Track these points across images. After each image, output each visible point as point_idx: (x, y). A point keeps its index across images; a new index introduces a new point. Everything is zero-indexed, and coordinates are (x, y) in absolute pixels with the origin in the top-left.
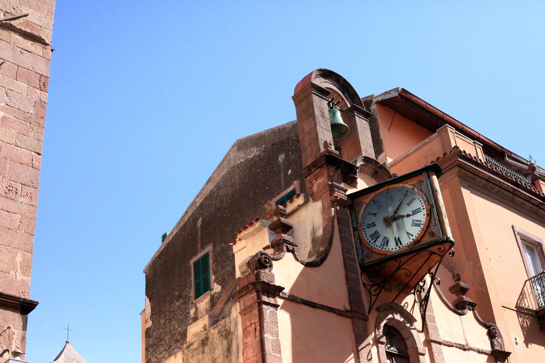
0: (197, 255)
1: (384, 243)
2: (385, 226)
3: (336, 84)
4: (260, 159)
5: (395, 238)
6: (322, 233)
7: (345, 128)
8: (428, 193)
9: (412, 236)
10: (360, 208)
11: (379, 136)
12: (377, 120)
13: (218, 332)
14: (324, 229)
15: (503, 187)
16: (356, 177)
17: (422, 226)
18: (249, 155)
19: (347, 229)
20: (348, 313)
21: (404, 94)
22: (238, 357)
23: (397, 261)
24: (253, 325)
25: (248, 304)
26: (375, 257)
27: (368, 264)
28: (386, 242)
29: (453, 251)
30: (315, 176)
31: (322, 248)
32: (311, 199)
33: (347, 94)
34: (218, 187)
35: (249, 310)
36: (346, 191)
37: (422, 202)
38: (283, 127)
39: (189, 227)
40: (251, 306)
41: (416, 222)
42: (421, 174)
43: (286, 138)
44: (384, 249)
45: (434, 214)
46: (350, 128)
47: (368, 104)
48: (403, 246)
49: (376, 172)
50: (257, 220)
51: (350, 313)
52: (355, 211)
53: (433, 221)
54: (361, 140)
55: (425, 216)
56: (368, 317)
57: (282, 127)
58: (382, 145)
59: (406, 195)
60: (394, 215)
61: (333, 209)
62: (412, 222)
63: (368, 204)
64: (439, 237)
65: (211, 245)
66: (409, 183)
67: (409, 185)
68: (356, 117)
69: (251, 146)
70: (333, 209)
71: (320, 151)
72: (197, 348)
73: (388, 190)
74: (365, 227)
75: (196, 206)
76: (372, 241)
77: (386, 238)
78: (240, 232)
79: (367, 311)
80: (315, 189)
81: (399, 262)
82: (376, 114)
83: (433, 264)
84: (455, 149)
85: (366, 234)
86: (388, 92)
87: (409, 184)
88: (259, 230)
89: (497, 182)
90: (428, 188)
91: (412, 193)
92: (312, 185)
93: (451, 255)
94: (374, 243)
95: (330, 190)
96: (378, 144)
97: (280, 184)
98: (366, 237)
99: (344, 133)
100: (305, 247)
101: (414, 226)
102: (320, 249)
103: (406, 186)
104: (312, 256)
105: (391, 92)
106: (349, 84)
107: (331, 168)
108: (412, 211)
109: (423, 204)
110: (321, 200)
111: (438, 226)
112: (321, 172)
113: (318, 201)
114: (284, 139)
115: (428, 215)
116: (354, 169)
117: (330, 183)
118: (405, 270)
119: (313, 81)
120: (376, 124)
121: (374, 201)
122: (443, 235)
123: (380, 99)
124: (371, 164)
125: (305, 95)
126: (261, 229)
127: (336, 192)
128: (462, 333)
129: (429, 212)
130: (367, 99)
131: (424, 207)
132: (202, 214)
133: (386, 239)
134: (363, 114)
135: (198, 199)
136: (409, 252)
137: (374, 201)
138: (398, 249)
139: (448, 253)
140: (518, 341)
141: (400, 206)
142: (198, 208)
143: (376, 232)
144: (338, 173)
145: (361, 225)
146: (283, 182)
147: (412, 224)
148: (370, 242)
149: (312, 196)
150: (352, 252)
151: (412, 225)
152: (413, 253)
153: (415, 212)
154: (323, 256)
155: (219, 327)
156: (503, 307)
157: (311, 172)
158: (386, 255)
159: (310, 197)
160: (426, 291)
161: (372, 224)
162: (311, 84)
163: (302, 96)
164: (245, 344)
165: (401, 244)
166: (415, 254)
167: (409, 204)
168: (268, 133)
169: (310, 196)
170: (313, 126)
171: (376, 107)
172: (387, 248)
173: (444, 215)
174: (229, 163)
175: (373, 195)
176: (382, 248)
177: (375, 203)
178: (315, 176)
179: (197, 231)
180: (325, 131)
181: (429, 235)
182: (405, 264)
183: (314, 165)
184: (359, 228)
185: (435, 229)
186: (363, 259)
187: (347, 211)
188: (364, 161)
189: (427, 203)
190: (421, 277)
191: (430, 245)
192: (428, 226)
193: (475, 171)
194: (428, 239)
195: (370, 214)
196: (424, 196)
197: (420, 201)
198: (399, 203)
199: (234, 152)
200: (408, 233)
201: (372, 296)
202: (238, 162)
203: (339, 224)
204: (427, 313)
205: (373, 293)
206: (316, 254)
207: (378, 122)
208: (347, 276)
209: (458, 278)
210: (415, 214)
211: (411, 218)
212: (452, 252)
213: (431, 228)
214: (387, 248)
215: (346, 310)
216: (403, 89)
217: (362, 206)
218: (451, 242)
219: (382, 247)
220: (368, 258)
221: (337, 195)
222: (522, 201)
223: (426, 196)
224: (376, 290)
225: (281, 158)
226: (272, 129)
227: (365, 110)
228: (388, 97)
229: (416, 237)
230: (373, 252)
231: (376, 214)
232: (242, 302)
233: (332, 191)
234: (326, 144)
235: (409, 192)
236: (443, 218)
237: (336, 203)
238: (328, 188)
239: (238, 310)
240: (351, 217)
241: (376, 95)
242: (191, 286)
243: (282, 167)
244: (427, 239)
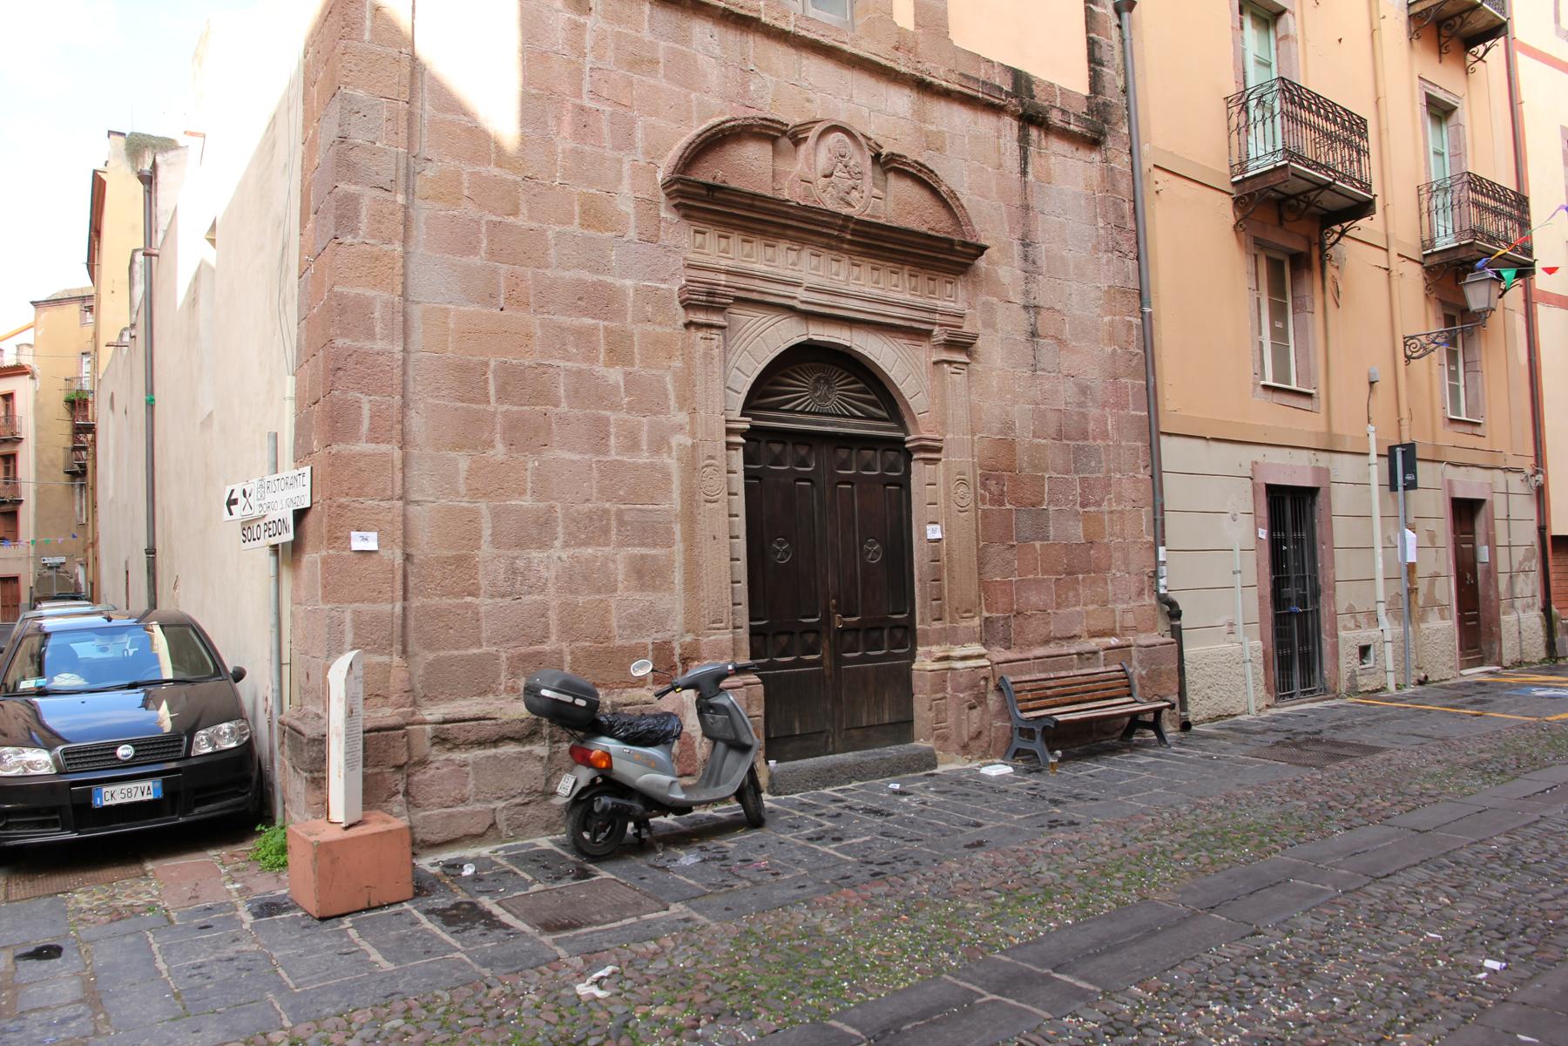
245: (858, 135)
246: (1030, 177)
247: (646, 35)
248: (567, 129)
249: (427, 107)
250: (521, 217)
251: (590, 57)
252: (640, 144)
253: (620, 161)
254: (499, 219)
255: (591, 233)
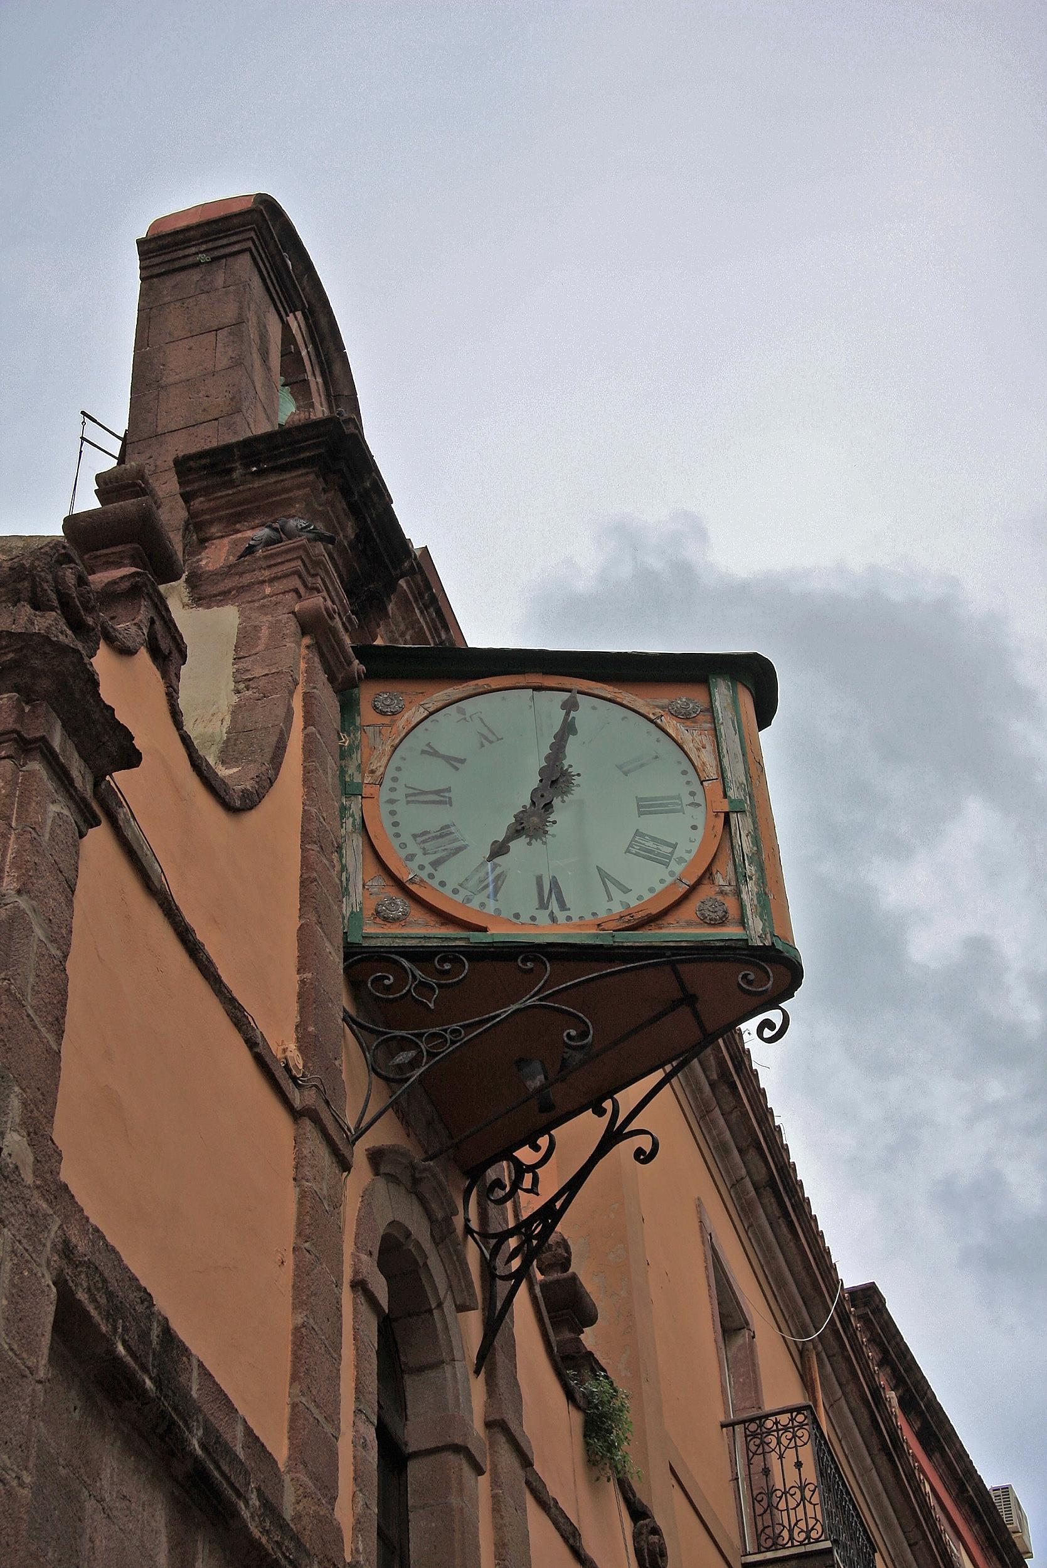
5: (539, 880)
9: (626, 891)
17: (678, 869)
30: (240, 504)
41: (651, 845)
48: (569, 918)
62: (633, 839)
74: (399, 795)
94: (429, 869)
98: (397, 835)
136: (601, 946)
137: (461, 711)
143: (444, 832)
147: (631, 845)
151: (628, 851)
158: (485, 930)
161: (438, 792)
165: (563, 906)
176: (469, 900)
177: (465, 719)
178: (240, 504)
200: (604, 876)
210: (651, 813)
229: (640, 898)
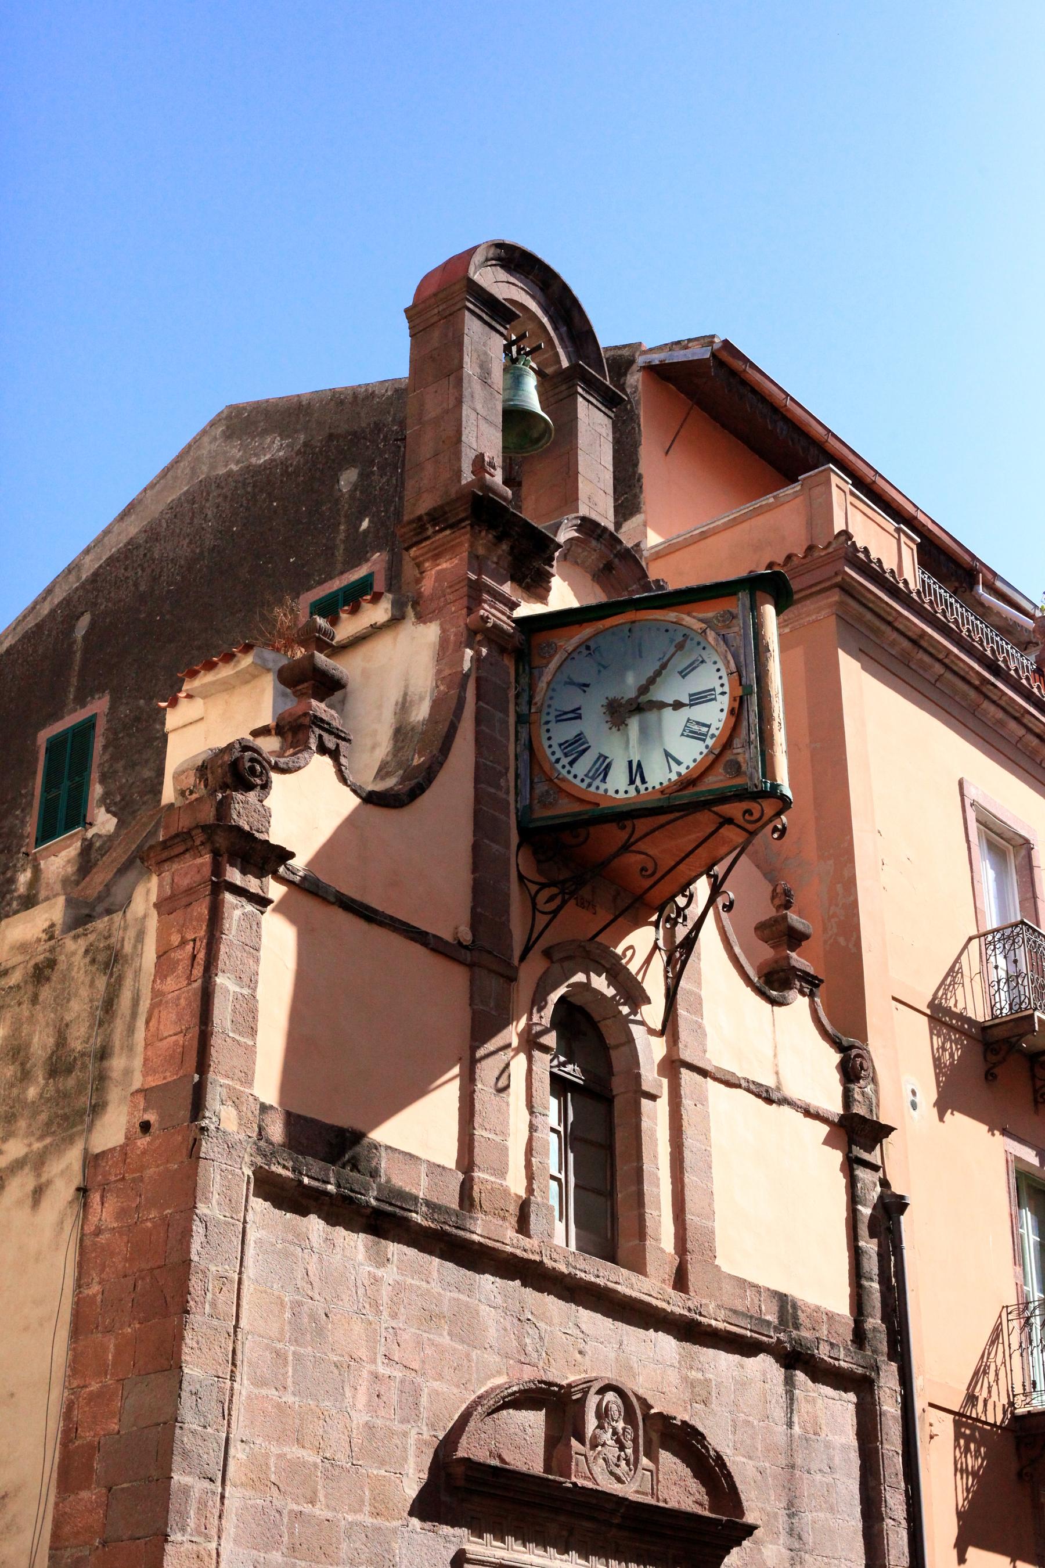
0: (62, 718)
1: (597, 770)
2: (609, 725)
3: (539, 294)
4: (285, 472)
5: (630, 763)
6: (427, 716)
7: (543, 425)
8: (742, 651)
9: (679, 763)
10: (545, 661)
11: (636, 465)
12: (638, 418)
13: (87, 952)
14: (436, 705)
15: (955, 668)
16: (549, 572)
17: (710, 742)
18: (256, 455)
19: (499, 715)
20: (463, 951)
21: (725, 357)
22: (131, 1030)
23: (624, 828)
24: (189, 947)
25: (185, 882)
26: (565, 807)
27: (539, 824)
28: (603, 768)
29: (783, 825)
30: (435, 549)
31: (420, 758)
32: (410, 613)
33: (564, 329)
34: (152, 534)
35: (184, 902)
36: (514, 606)
37: (723, 673)
38: (366, 390)
39: (49, 635)
40: (190, 891)
41: (696, 728)
42: (735, 594)
43: (369, 424)
44: (592, 789)
45: (751, 713)
46: (558, 430)
47: (620, 368)
48: (647, 789)
49: (609, 567)
50: (247, 648)
51: (468, 952)
52: (531, 668)
53: (744, 731)
54: (580, 469)
55: (723, 716)
56: (517, 969)
57: (363, 390)
58: (641, 492)
59: (680, 647)
60: (637, 697)
61: (469, 653)
63: (569, 654)
64: (751, 778)
65: (107, 698)
66: (694, 614)
67: (695, 621)
68: (580, 399)
69: (265, 432)
70: (469, 653)
71: (459, 481)
72: (18, 987)
73: (633, 622)
74: (551, 718)
75: (79, 578)
76: (565, 761)
77: (606, 758)
78: (193, 674)
79: (517, 953)
80: (428, 585)
81: (629, 830)
82: (638, 403)
83: (723, 851)
84: (843, 538)
85: (549, 738)
86: (683, 344)
87: (694, 617)
88: (248, 678)
89: (940, 652)
90: (746, 635)
91: (699, 643)
92: (422, 573)
93: (776, 836)
94: (568, 767)
95: (469, 597)
96: (630, 487)
97: (333, 554)
98: (550, 746)
99: (538, 440)
100: (374, 748)
101: (688, 736)
102: (413, 760)
103: (688, 620)
104: (388, 774)
105: (690, 345)
106: (575, 301)
107: (483, 533)
108: (690, 695)
109: (725, 680)
110: (438, 622)
111: (755, 749)
112: (453, 540)
113: (431, 622)
114: (364, 425)
115: (732, 711)
116: (548, 547)
117: (474, 577)
118: (643, 856)
119: (475, 273)
120: (633, 428)
121: (588, 648)
122: (764, 775)
123: (656, 358)
124: (598, 540)
125: (444, 310)
126: (254, 677)
127: (486, 606)
128: (771, 1054)
129: (736, 705)
130: (620, 352)
131: (726, 689)
132: (95, 604)
133: (604, 761)
134: (599, 395)
135: (88, 559)
137: (588, 648)
138: (633, 793)
139: (770, 827)
140: (917, 1100)
141: (658, 673)
142: (83, 586)
143: (579, 738)
144: (500, 552)
145: (540, 712)
146: (341, 551)
148: (558, 761)
149: (415, 604)
150: (502, 782)
151: (682, 735)
152: (671, 812)
153: (698, 699)
154: (420, 779)
155: (92, 937)
156: (894, 999)
157: (424, 535)
158: (598, 805)
159: (409, 607)
160: (690, 924)
161: (573, 711)
162: (465, 282)
163: (436, 311)
164: (156, 994)
165: (643, 781)
166: (677, 814)
167: (684, 674)
168: (322, 401)
169: (410, 604)
170: (451, 406)
171: (643, 383)
172: (603, 787)
173: (777, 720)
174: (193, 469)
175: (587, 631)
176: (589, 785)
178: (435, 549)
179: (70, 652)
180: (484, 426)
181: (725, 769)
182: (646, 840)
183: (438, 517)
184: (533, 718)
185: (746, 755)
186: (530, 808)
187: (509, 663)
188: (579, 528)
189: (737, 678)
190: (683, 881)
191: (723, 798)
192: (727, 745)
193: (885, 611)
194: (721, 781)
195: (571, 683)
196: (730, 657)
197: (718, 670)
198: (657, 666)
199: (215, 439)
200: (667, 754)
201: (537, 913)
202: (222, 471)
203: (479, 697)
204: (682, 983)
205: (540, 906)
206: (401, 772)
207: (639, 426)
208: (476, 848)
209: (785, 900)
211: (685, 713)
212: (780, 826)
213: (735, 751)
214: (603, 787)
215: (460, 943)
216: (726, 343)
217: (552, 657)
218: (783, 798)
219: (590, 780)
220: (545, 806)
221: (486, 614)
222: (1000, 715)
223: (735, 657)
224: (551, 899)
225: (348, 479)
226: (333, 391)
227: (608, 383)
228: (679, 356)
229: (688, 767)
230: (561, 790)
231: (587, 685)
232: (167, 875)
233: (474, 599)
234: (480, 464)
235: (692, 639)
236: (772, 729)
237: (479, 637)
238: (465, 589)
239: (153, 898)
240: (517, 681)
241: (647, 345)
242: (30, 804)
243: (346, 506)
244: (717, 780)
245: (630, 1394)
246: (797, 1429)
247: (436, 1288)
248: (362, 1399)
249: (245, 1382)
250: (318, 1505)
251: (385, 1315)
252: (425, 1414)
253: (405, 1434)
254: (300, 1508)
255: (378, 1522)
